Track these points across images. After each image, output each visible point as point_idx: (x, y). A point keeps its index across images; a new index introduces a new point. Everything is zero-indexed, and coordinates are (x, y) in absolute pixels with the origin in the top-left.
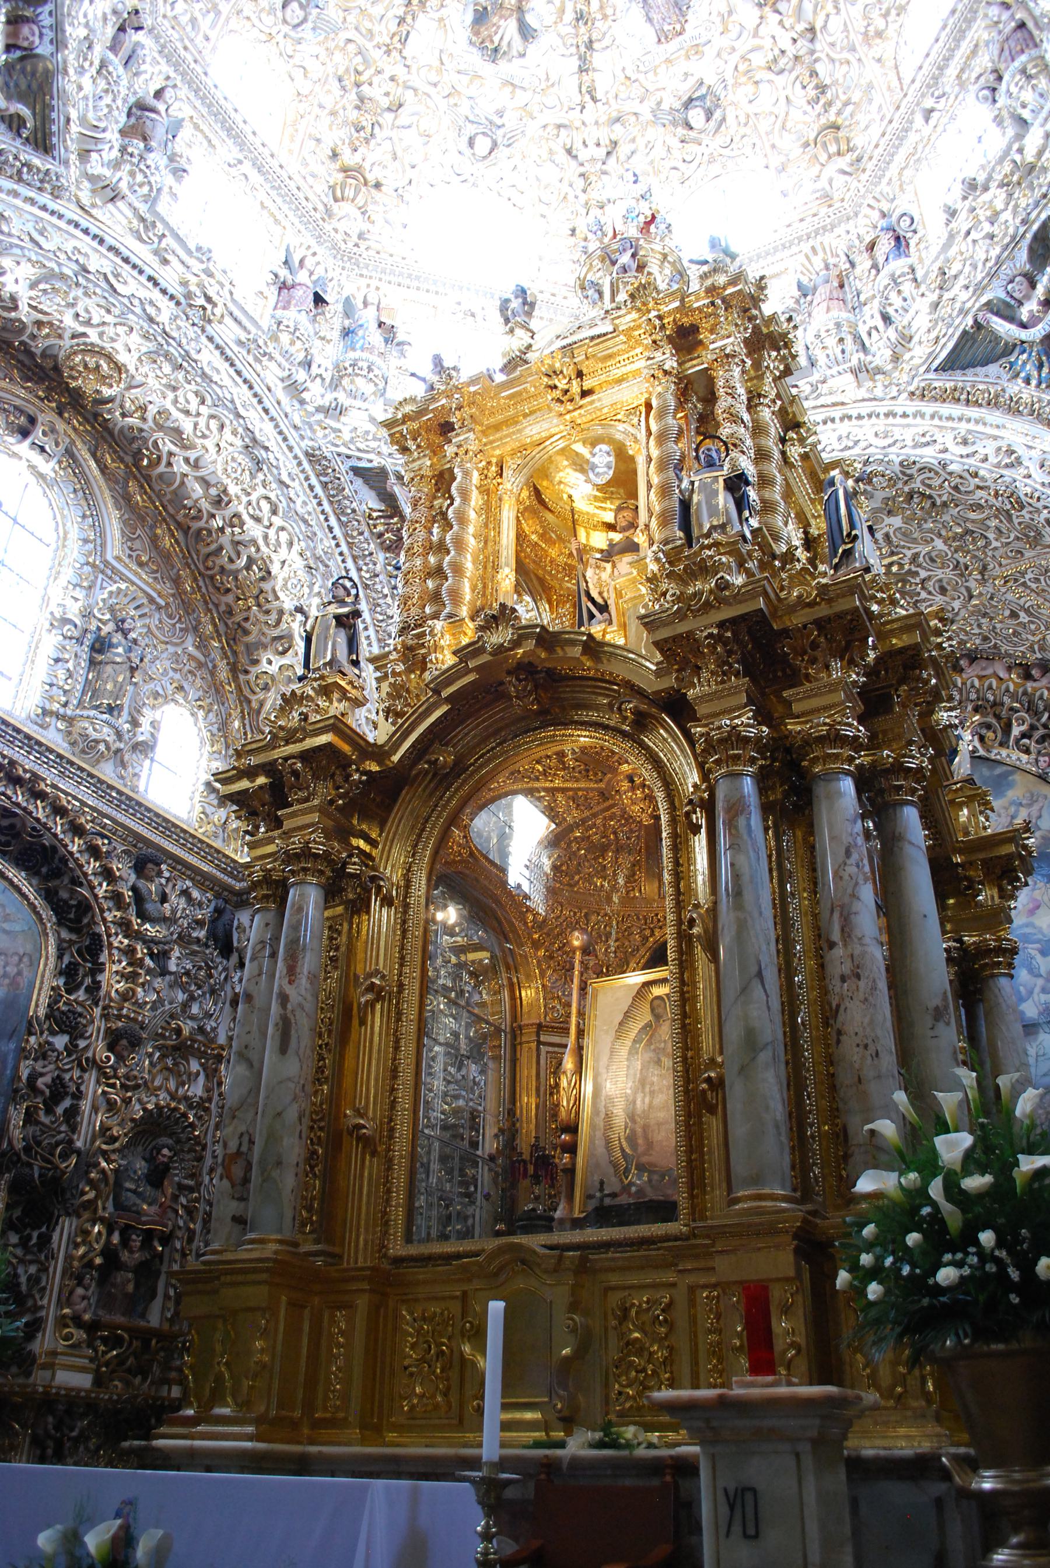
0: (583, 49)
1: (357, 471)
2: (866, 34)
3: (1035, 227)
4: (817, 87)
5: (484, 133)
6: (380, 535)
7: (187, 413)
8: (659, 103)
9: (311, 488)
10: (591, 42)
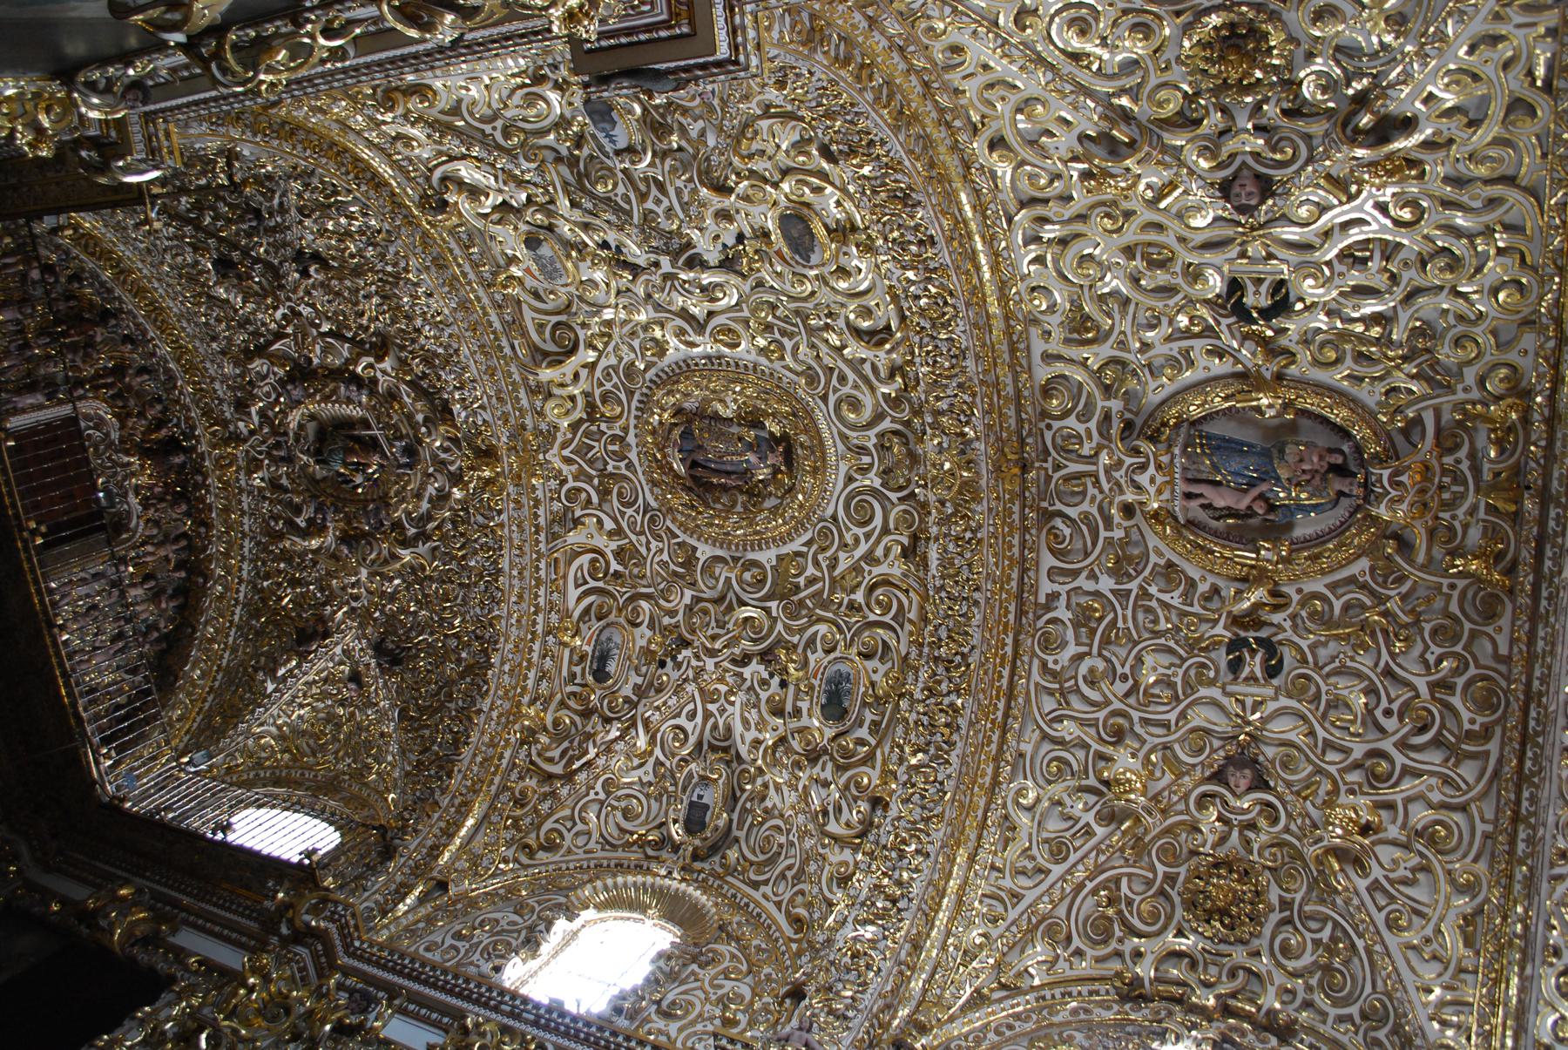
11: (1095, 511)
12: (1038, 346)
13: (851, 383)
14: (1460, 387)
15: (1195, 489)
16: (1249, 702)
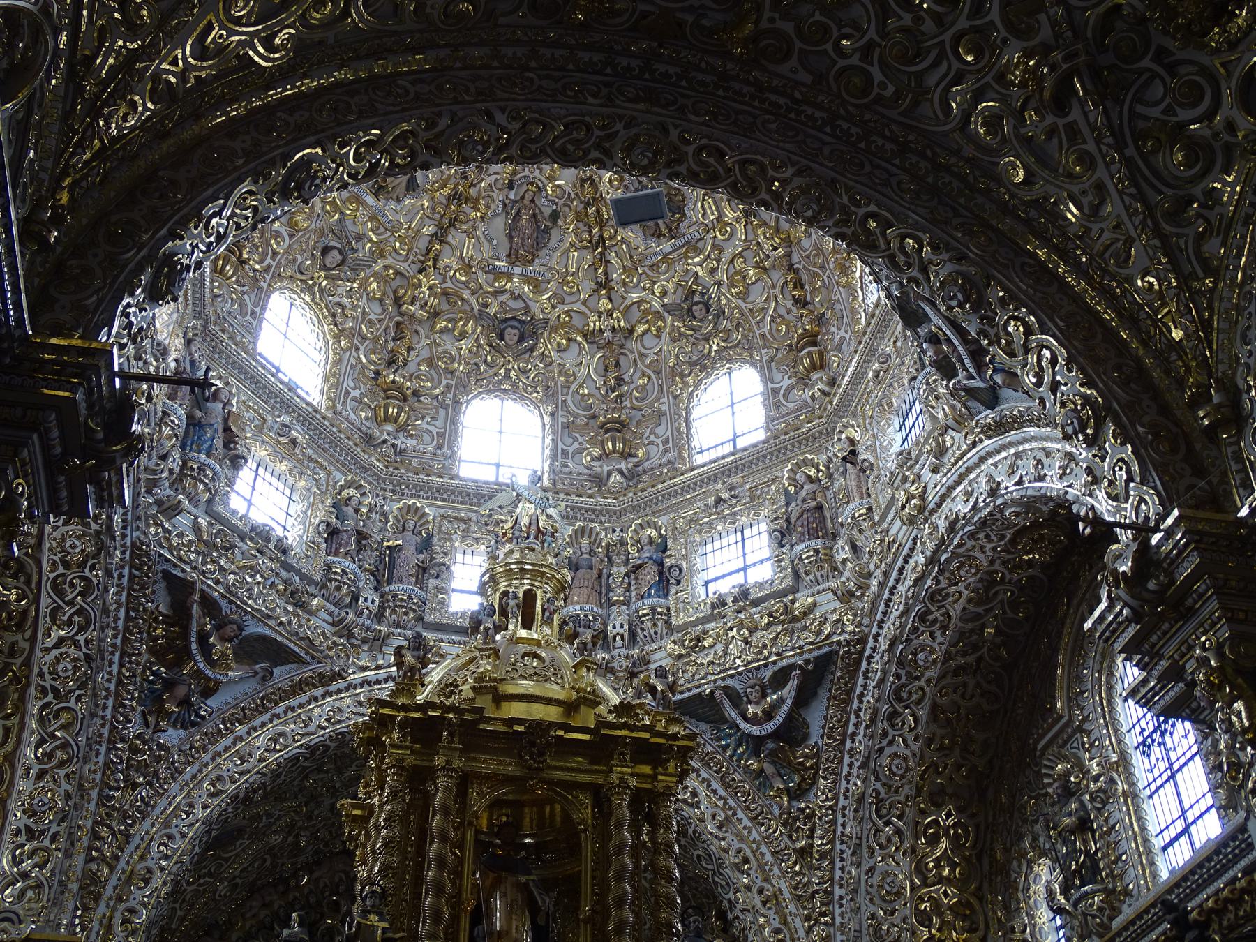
0: (446, 222)
1: (167, 575)
2: (673, 368)
4: (616, 379)
5: (340, 252)
6: (157, 638)
8: (486, 305)
9: (121, 576)
10: (455, 219)
14: (777, 16)
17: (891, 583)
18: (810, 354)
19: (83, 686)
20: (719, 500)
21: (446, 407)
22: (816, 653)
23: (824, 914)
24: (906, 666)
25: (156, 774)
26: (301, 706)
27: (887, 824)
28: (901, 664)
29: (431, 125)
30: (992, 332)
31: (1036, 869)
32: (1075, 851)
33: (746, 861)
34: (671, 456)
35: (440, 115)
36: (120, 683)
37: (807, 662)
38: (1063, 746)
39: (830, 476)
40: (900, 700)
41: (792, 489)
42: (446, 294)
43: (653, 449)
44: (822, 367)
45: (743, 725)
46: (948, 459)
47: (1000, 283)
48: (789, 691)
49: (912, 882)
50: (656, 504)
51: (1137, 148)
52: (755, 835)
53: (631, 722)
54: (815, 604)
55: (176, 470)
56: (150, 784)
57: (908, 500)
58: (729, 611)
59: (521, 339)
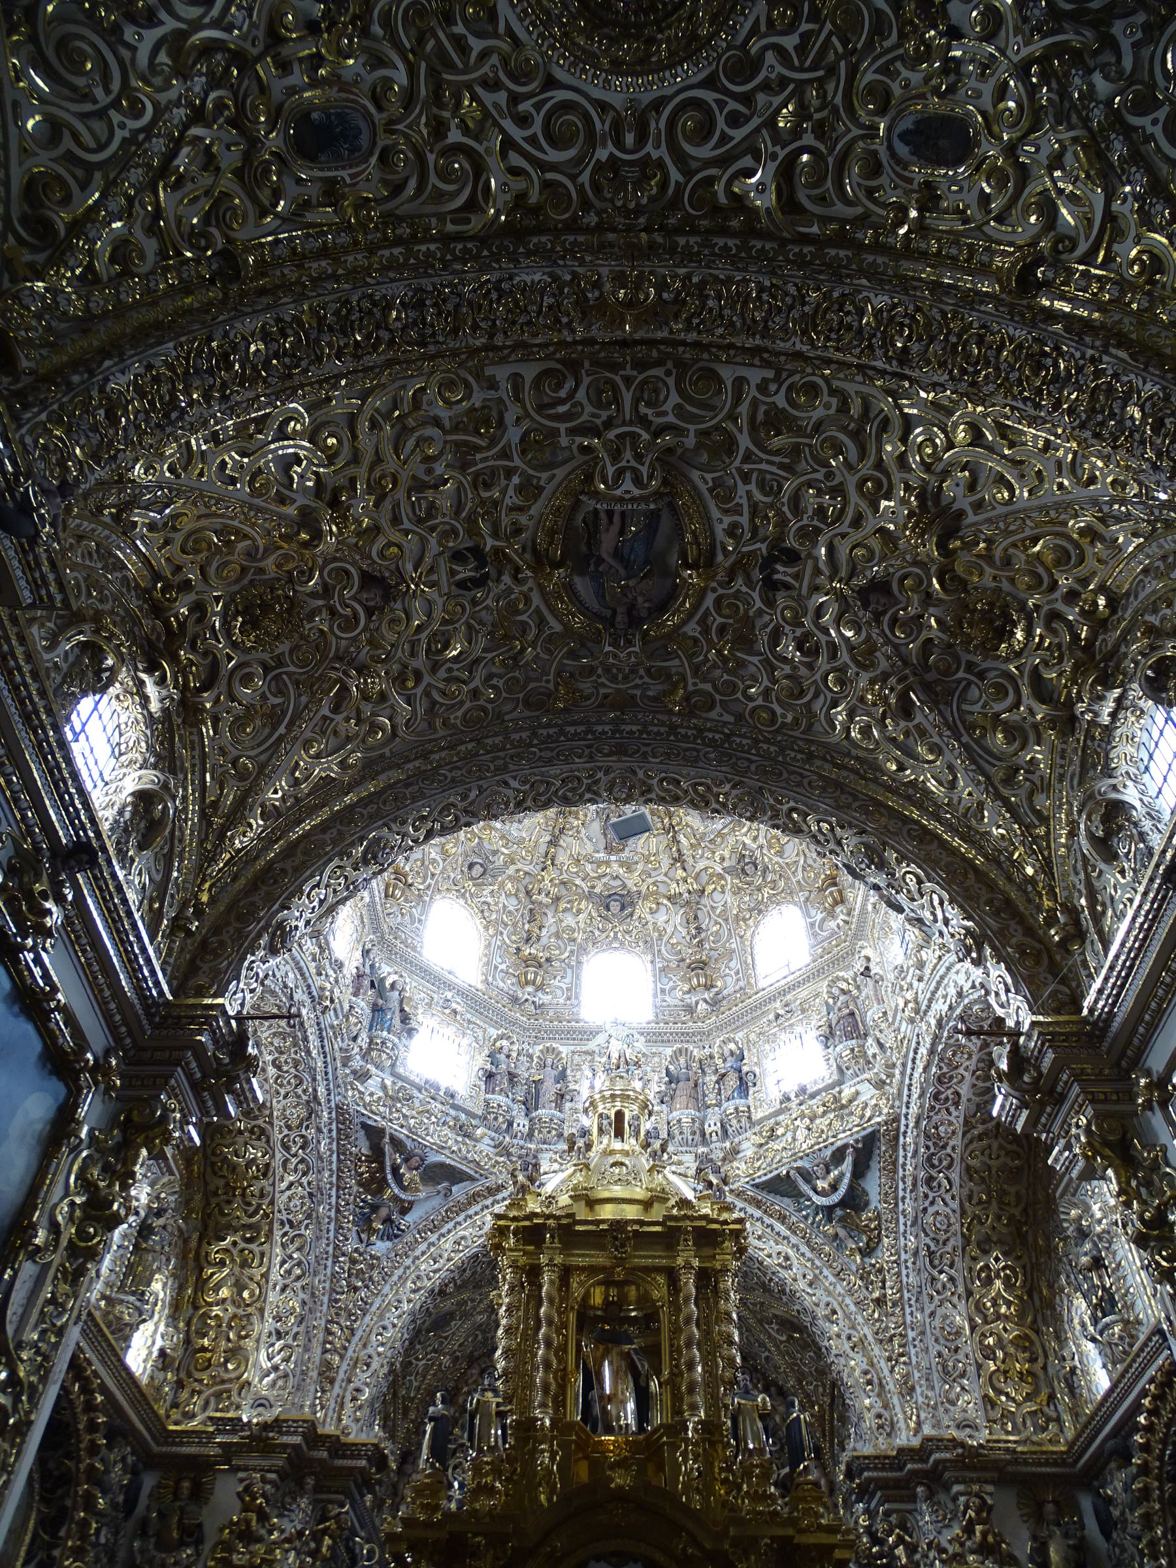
1: (364, 1126)
3: (839, 1143)
7: (279, 1068)
8: (593, 887)
9: (330, 1131)
11: (584, 417)
12: (755, 376)
13: (730, 132)
15: (617, 519)
16: (434, 577)
17: (909, 1071)
18: (831, 893)
19: (309, 1217)
20: (777, 1016)
21: (571, 967)
22: (863, 1133)
23: (902, 1355)
24: (934, 1140)
25: (371, 1278)
26: (476, 1214)
27: (941, 1272)
28: (928, 1137)
29: (464, 797)
30: (896, 884)
31: (1075, 1302)
32: (1094, 1286)
33: (834, 1312)
34: (741, 984)
35: (470, 790)
36: (338, 1211)
37: (857, 1141)
38: (1073, 1195)
39: (858, 988)
40: (933, 1166)
41: (831, 1001)
42: (563, 883)
43: (728, 979)
44: (842, 902)
45: (815, 1198)
46: (927, 971)
47: (893, 848)
48: (847, 1166)
49: (971, 1320)
50: (735, 1023)
51: (970, 736)
52: (839, 1289)
53: (690, 1213)
54: (857, 1093)
55: (365, 1046)
56: (367, 1287)
57: (906, 1004)
58: (793, 1105)
59: (623, 908)
